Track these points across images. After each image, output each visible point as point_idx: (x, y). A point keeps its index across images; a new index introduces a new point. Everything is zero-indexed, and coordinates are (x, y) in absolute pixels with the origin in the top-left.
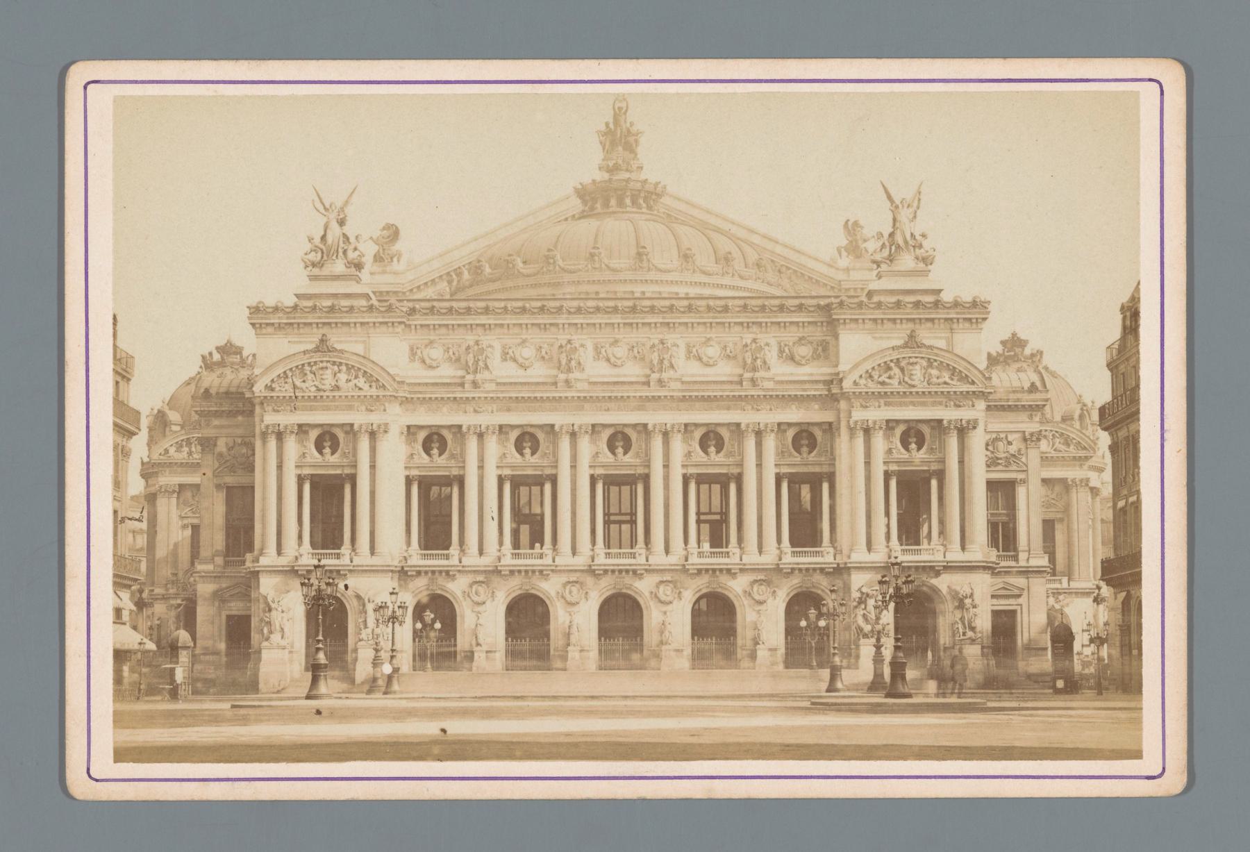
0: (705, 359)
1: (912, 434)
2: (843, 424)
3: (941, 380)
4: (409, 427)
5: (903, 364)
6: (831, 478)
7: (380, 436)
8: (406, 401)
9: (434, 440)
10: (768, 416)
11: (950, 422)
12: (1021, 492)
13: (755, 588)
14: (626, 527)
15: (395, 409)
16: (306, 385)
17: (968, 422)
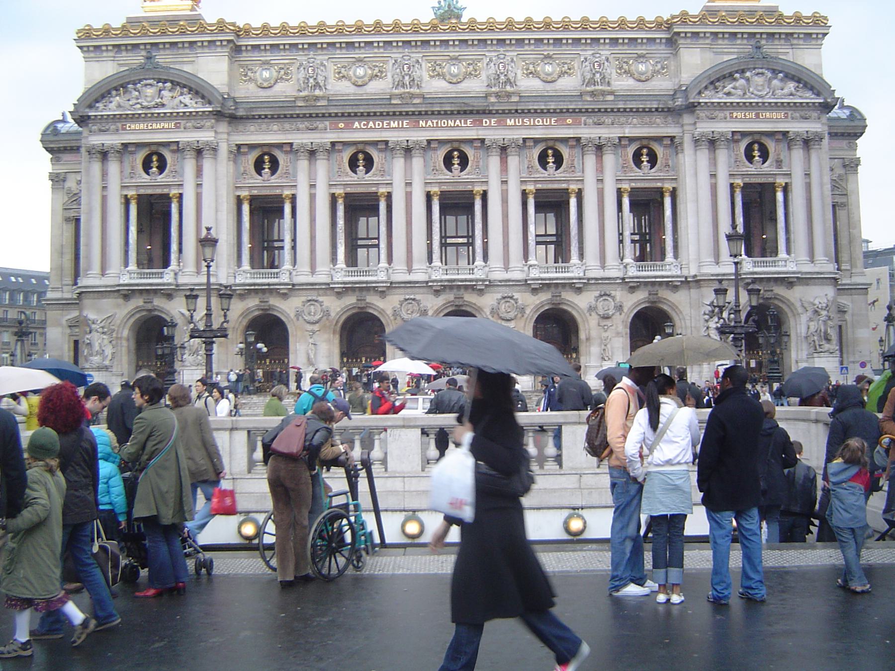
0: (542, 76)
1: (756, 147)
2: (687, 139)
3: (786, 91)
4: (239, 146)
5: (748, 74)
6: (674, 194)
7: (206, 154)
8: (234, 119)
9: (266, 160)
10: (608, 132)
11: (797, 134)
12: (842, 214)
13: (600, 305)
14: (463, 250)
15: (223, 127)
16: (131, 103)
17: (816, 134)
